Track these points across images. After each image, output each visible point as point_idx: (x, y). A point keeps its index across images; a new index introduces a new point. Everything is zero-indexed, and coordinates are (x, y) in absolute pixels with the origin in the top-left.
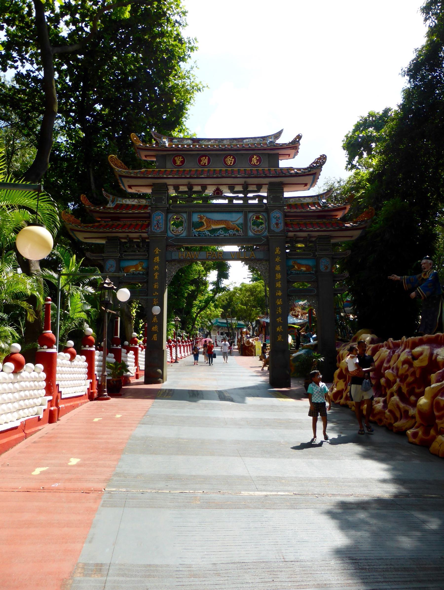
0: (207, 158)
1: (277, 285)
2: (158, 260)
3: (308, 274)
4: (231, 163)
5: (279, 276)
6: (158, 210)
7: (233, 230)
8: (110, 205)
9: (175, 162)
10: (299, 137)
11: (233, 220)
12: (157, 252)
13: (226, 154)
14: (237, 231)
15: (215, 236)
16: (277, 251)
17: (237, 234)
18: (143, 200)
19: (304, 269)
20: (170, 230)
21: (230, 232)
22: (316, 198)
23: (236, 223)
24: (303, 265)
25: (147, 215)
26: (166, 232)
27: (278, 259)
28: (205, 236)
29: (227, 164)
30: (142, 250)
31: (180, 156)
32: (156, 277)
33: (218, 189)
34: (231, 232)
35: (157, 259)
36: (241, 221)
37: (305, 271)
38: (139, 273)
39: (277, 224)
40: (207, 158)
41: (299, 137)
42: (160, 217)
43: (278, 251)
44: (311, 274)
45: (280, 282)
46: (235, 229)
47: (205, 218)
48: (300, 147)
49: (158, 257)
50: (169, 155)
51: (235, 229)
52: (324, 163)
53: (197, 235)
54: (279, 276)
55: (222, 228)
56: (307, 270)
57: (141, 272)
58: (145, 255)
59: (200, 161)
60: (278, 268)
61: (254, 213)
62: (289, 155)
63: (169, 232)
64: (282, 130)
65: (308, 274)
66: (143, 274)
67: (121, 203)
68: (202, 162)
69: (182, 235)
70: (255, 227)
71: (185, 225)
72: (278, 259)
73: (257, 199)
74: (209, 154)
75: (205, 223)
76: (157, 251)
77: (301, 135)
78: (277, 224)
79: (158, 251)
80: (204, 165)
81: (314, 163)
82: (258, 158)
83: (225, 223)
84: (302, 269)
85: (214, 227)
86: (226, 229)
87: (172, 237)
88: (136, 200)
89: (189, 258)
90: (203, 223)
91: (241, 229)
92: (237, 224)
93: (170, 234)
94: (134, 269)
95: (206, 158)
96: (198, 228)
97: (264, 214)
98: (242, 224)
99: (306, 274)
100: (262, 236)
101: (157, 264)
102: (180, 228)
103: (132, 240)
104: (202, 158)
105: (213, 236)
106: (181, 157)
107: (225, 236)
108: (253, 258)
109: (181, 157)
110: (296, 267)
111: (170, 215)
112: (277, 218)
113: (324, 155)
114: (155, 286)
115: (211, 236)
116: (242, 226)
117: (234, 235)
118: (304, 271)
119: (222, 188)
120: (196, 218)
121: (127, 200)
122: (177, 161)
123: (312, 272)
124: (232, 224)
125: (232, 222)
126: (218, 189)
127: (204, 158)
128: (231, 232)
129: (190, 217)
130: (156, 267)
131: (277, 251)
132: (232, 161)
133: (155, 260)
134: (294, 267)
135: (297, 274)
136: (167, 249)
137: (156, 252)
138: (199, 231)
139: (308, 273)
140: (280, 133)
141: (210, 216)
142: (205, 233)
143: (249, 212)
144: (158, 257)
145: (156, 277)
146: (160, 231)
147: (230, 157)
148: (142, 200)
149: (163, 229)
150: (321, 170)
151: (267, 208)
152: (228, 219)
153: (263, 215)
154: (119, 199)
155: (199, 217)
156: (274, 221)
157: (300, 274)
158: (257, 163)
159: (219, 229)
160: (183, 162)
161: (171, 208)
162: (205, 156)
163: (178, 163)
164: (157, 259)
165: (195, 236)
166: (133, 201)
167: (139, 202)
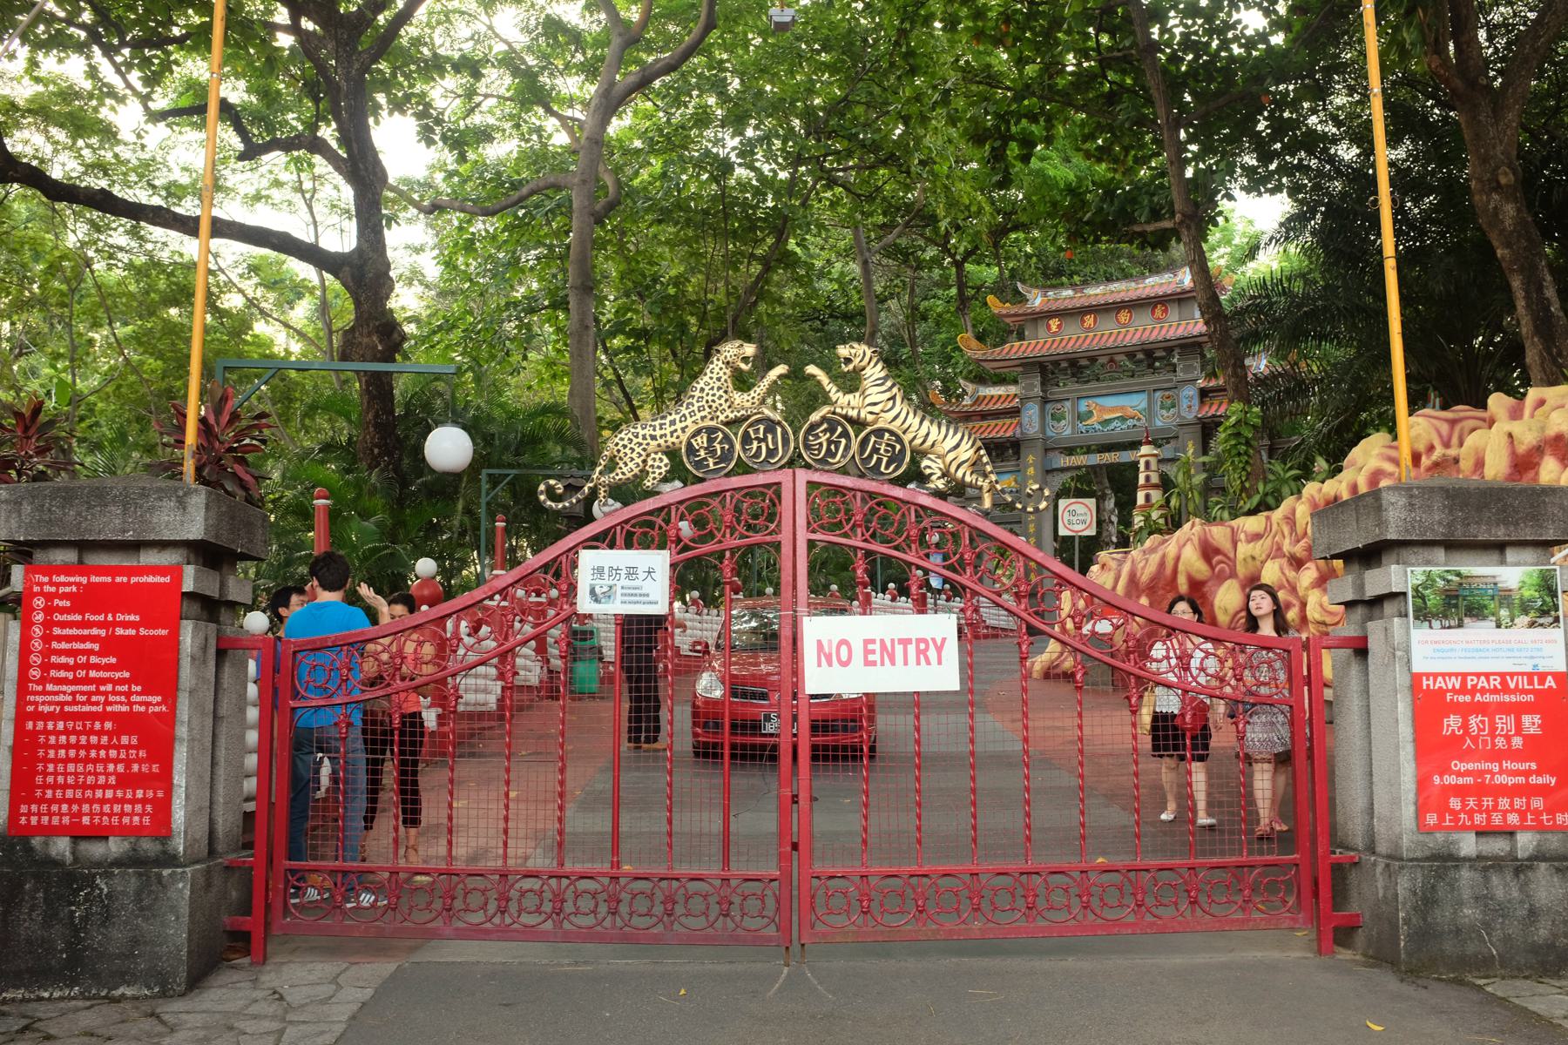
8: (967, 401)
9: (1049, 327)
33: (1112, 360)
34: (1130, 422)
35: (1031, 471)
36: (1144, 405)
59: (1083, 321)
70: (1164, 412)
71: (1068, 416)
76: (1031, 459)
85: (1107, 417)
86: (1123, 419)
93: (1049, 433)
111: (1048, 406)
119: (1118, 358)
120: (1083, 406)
128: (1130, 422)
141: (1100, 401)
156: (1185, 403)
160: (1059, 326)
162: (1090, 312)
163: (1054, 328)
164: (1031, 471)
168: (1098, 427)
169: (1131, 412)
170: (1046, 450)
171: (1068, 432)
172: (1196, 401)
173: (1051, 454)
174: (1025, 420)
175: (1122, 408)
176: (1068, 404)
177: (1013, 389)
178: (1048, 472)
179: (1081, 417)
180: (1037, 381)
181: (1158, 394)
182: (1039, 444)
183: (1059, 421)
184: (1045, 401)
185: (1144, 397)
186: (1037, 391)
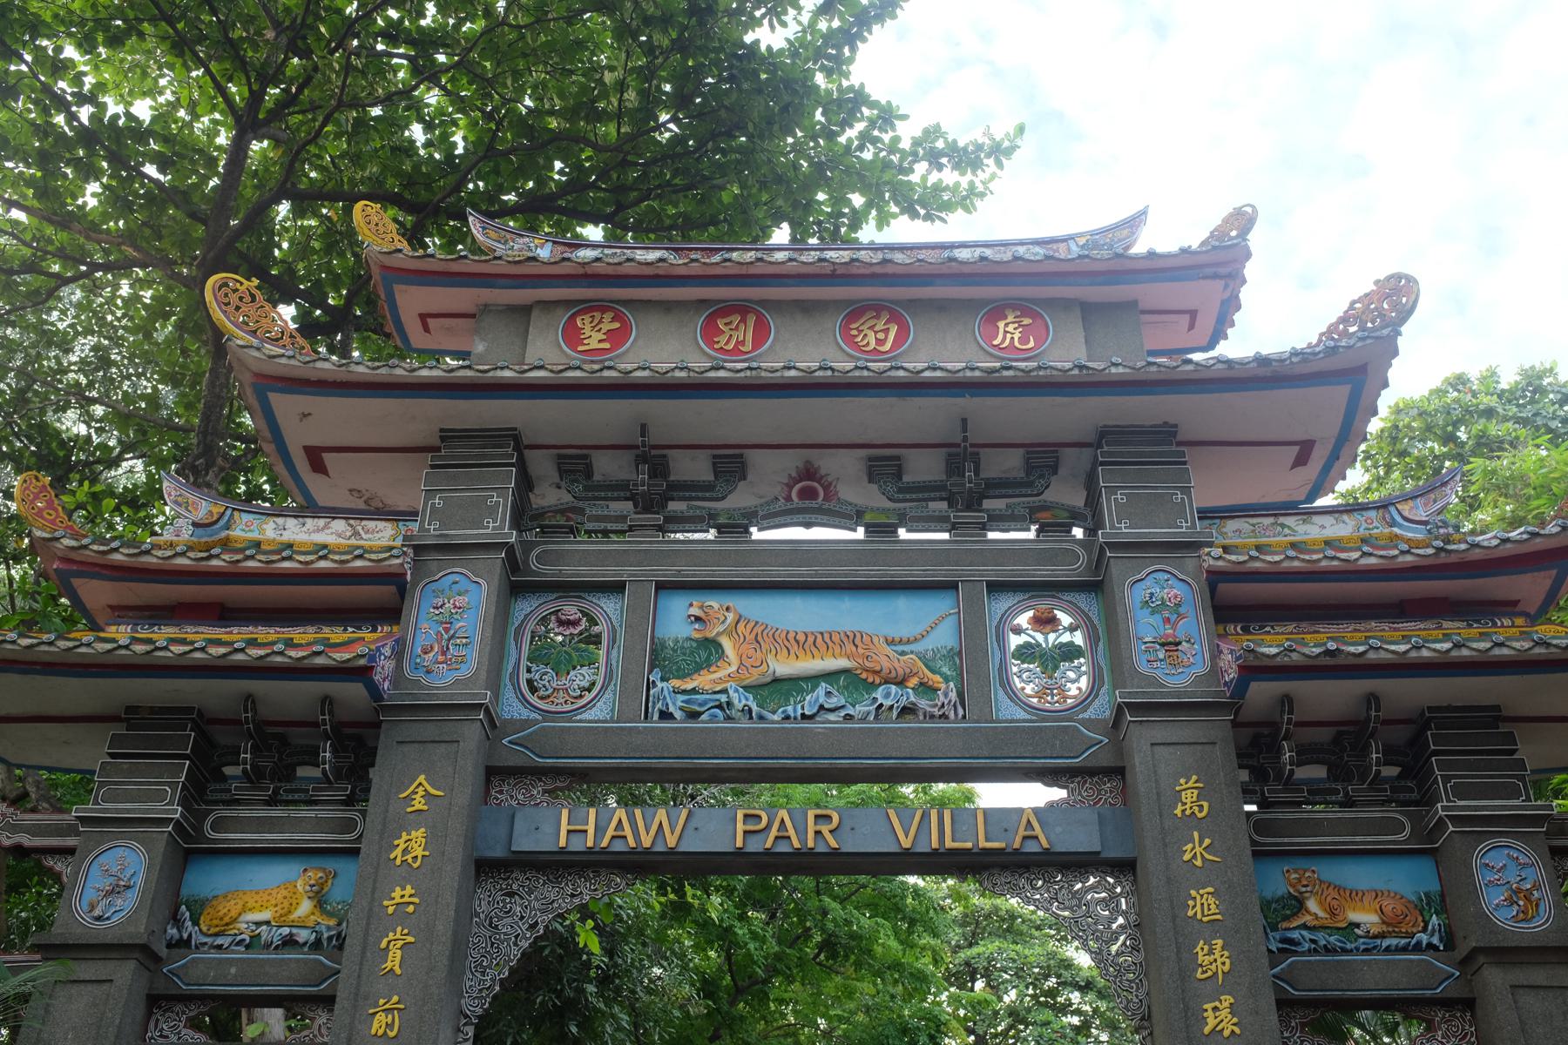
0: (751, 319)
1: (1211, 1022)
2: (419, 852)
3: (1404, 949)
4: (880, 342)
5: (1213, 958)
6: (454, 563)
7: (901, 683)
10: (1243, 220)
11: (904, 631)
12: (419, 803)
13: (849, 302)
14: (926, 689)
15: (787, 718)
16: (1189, 797)
17: (923, 704)
18: (381, 525)
19: (1366, 918)
20: (517, 688)
21: (879, 694)
22: (1373, 514)
23: (918, 647)
24: (1355, 896)
25: (385, 592)
26: (495, 686)
27: (1195, 850)
28: (729, 718)
29: (856, 346)
30: (325, 795)
31: (603, 310)
32: (394, 960)
33: (809, 473)
34: (887, 696)
36: (944, 637)
37: (1382, 936)
38: (289, 942)
39: (1171, 645)
40: (751, 319)
41: (1243, 220)
42: (461, 600)
43: (1189, 798)
44: (1418, 948)
45: (1227, 1000)
46: (913, 682)
47: (731, 617)
48: (1250, 270)
49: (419, 834)
50: (548, 305)
51: (913, 682)
52: (1406, 313)
53: (678, 714)
54: (1213, 958)
55: (830, 676)
56: (1392, 925)
57: (303, 935)
58: (349, 825)
60: (1203, 904)
61: (1020, 596)
62: (1193, 314)
63: (508, 694)
64: (1143, 213)
65: (1404, 949)
66: (317, 945)
67: (254, 535)
68: (723, 339)
69: (588, 715)
72: (1195, 850)
73: (1034, 528)
74: (764, 303)
75: (727, 644)
76: (420, 792)
77: (1249, 210)
78: (1171, 645)
79: (427, 795)
80: (736, 351)
81: (1344, 319)
82: (1027, 321)
83: (850, 647)
84: (1354, 916)
85: (783, 666)
86: (851, 681)
87: (527, 723)
88: (339, 525)
89: (618, 847)
90: (719, 646)
91: (947, 679)
92: (922, 657)
93: (511, 708)
94: (265, 915)
95: (743, 321)
96: (683, 676)
97: (1082, 600)
98: (953, 655)
99: (1388, 950)
100: (1083, 722)
101: (408, 873)
102: (582, 676)
103: (283, 740)
104: (721, 324)
105: (776, 717)
106: (608, 316)
107: (848, 717)
108: (1031, 847)
109: (612, 315)
110: (1312, 905)
111: (524, 607)
112: (1168, 611)
113: (1398, 277)
114: (379, 1023)
115: (761, 718)
116: (953, 667)
117: (908, 711)
118: (1367, 935)
119: (829, 463)
121: (291, 522)
122: (587, 331)
123: (1424, 938)
124: (888, 650)
125: (891, 642)
126: (809, 473)
127: (736, 319)
128: (887, 696)
129: (643, 619)
130: (397, 893)
131: (1189, 797)
132: (886, 331)
133: (398, 852)
134: (1299, 905)
135: (1328, 950)
136: (487, 792)
137: (409, 799)
138: (694, 691)
139: (1394, 942)
140: (1134, 223)
142: (729, 704)
143: (996, 588)
144: (419, 834)
145: (394, 960)
146: (450, 677)
147: (877, 317)
148: (371, 524)
149: (466, 671)
150: (1395, 353)
151: (1099, 564)
152: (867, 627)
153: (1072, 609)
154: (245, 517)
155: (695, 611)
156: (1145, 627)
157: (1345, 951)
158: (1024, 340)
159: (815, 679)
161: (534, 565)
162: (741, 309)
163: (594, 340)
164: (413, 844)
165: (666, 715)
166: (318, 531)
167: (356, 534)
168: (739, 700)
169: (886, 658)
170: (495, 774)
171: (600, 712)
172: (1193, 626)
173: (509, 796)
174: (423, 626)
175: (852, 638)
176: (609, 608)
177: (381, 534)
178: (486, 868)
179: (661, 658)
180: (502, 502)
181: (1003, 603)
182: (471, 734)
183: (563, 665)
184: (518, 584)
185: (937, 607)
186: (497, 526)
